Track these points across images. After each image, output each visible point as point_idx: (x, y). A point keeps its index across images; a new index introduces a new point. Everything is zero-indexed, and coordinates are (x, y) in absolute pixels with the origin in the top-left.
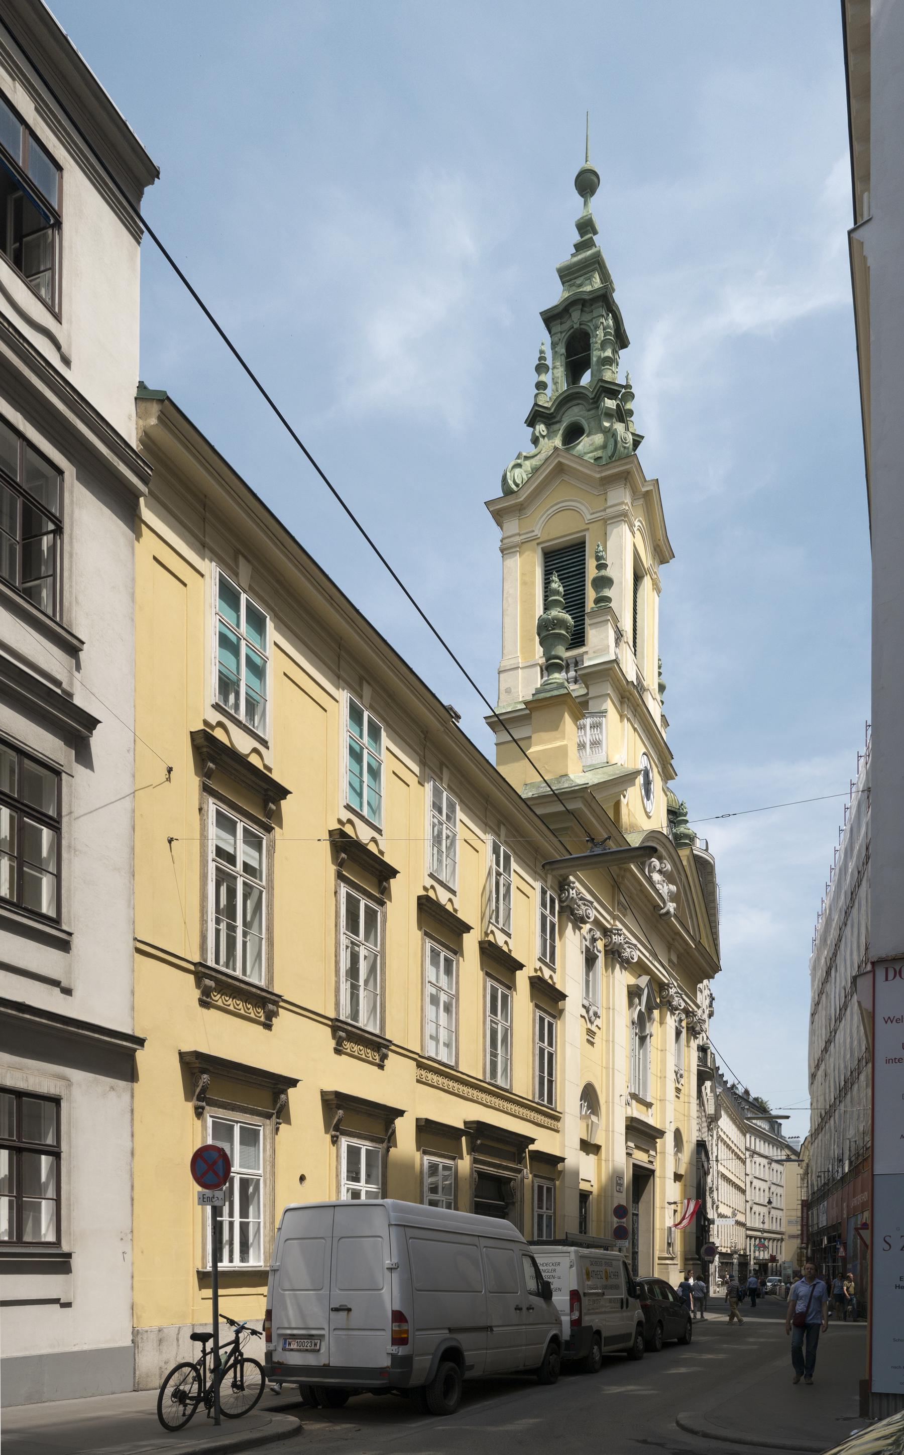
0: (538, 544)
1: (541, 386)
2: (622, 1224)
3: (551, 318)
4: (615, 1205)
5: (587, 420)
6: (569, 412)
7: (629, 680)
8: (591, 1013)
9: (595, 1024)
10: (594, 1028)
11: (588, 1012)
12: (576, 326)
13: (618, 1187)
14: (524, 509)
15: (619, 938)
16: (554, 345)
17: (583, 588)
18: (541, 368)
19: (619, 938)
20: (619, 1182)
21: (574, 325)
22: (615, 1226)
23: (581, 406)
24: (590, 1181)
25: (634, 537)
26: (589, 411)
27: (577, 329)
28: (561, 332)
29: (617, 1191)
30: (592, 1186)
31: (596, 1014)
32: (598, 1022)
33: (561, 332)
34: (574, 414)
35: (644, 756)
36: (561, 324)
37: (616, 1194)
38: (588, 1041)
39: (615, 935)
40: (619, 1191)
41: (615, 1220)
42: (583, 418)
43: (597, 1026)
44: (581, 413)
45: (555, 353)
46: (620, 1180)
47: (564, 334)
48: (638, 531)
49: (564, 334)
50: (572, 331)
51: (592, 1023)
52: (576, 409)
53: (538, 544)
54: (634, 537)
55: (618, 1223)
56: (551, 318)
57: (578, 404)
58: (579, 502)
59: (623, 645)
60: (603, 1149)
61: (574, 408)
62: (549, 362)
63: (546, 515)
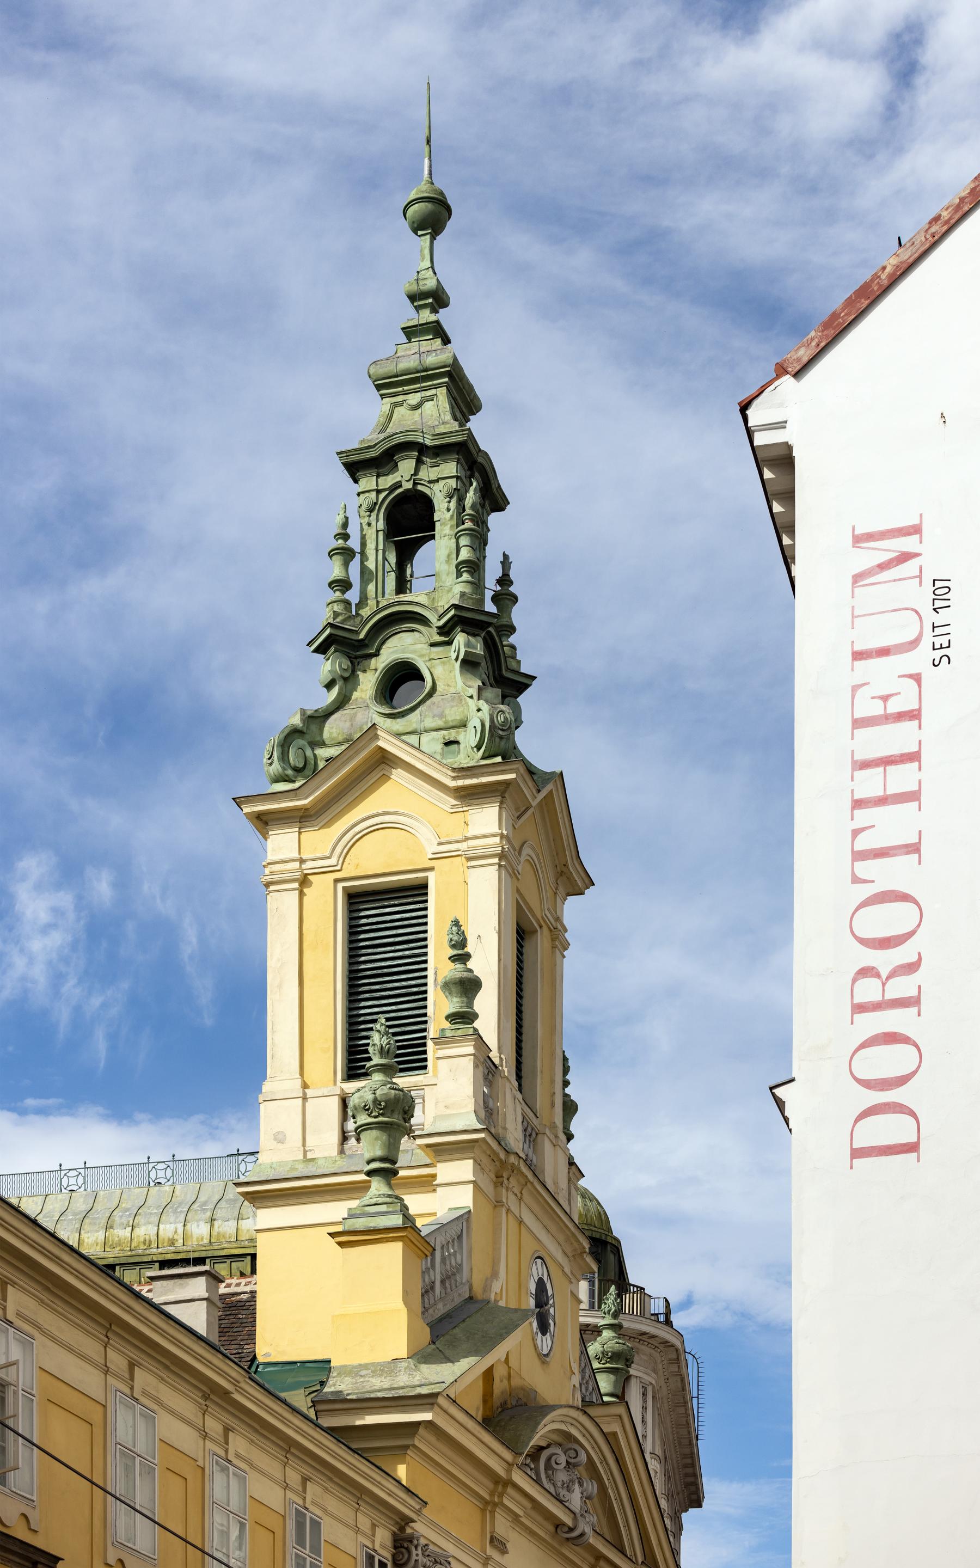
12: (408, 485)
17: (423, 966)
21: (404, 483)
33: (379, 492)
35: (539, 1261)
36: (378, 476)
47: (384, 494)
49: (384, 494)
57: (413, 631)
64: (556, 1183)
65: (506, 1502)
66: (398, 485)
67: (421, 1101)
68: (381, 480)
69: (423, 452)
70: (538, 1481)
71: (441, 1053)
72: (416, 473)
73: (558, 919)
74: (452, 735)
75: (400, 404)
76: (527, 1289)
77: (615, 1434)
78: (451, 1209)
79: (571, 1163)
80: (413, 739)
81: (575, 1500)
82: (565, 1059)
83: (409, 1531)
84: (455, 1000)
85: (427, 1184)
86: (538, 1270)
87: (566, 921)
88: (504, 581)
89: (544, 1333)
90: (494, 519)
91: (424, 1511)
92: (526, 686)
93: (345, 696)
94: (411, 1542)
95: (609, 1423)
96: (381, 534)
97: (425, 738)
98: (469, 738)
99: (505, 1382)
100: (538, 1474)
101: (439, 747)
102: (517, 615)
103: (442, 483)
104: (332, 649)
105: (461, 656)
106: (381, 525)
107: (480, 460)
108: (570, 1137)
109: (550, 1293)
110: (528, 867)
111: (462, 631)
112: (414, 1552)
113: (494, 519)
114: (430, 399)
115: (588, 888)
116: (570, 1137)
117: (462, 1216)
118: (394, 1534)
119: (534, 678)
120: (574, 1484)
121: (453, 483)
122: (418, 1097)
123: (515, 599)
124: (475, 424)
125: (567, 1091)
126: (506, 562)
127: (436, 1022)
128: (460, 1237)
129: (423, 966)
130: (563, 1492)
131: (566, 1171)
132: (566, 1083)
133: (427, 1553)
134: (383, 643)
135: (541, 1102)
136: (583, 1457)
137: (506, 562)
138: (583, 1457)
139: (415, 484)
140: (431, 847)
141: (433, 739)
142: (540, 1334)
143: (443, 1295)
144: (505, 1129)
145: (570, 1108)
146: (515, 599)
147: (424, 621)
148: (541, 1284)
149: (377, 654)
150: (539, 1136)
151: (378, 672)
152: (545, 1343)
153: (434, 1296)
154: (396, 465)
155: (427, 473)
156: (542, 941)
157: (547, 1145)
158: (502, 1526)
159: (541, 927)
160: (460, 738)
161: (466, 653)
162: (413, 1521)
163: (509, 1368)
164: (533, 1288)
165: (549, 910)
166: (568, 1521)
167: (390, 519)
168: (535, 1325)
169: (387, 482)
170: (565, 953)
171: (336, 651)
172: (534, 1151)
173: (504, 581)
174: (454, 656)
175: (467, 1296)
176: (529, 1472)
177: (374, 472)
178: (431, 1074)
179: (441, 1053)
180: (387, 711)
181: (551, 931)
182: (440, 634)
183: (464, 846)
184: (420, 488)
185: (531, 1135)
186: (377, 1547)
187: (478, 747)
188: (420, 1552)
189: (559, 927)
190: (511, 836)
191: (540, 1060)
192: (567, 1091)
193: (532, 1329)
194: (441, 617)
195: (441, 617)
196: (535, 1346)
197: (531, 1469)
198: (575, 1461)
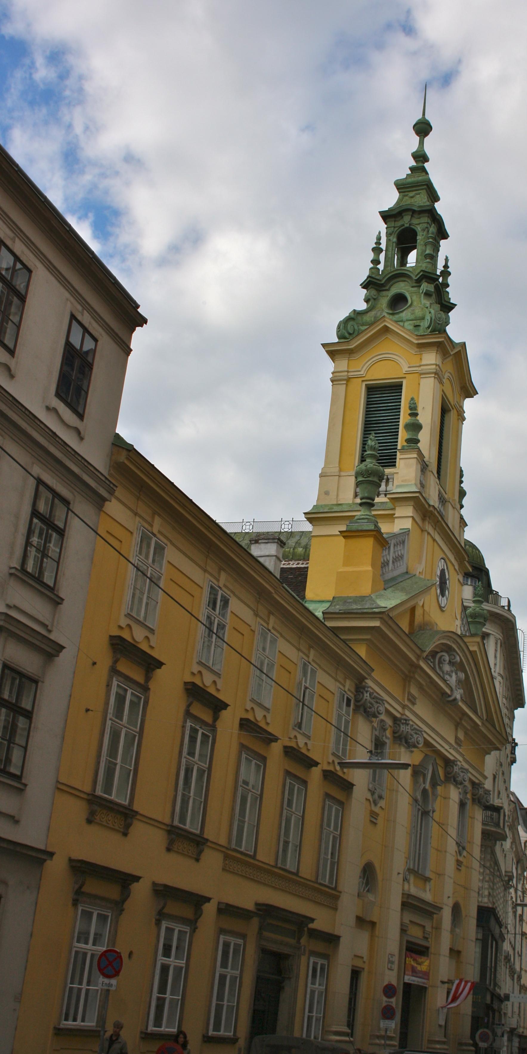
0: (363, 381)
1: (376, 262)
2: (390, 1004)
3: (386, 216)
4: (386, 983)
5: (411, 293)
6: (396, 285)
7: (431, 503)
8: (376, 796)
9: (379, 805)
10: (377, 810)
11: (373, 793)
12: (407, 225)
13: (390, 965)
14: (354, 353)
15: (407, 727)
16: (388, 235)
17: (398, 420)
18: (377, 250)
19: (407, 727)
20: (391, 959)
22: (384, 1004)
23: (406, 283)
24: (362, 958)
25: (443, 391)
26: (413, 287)
27: (407, 227)
28: (394, 227)
29: (388, 969)
30: (364, 962)
31: (381, 797)
32: (382, 803)
33: (394, 227)
34: (400, 287)
35: (443, 561)
36: (395, 221)
37: (387, 972)
38: (371, 821)
39: (403, 724)
40: (391, 969)
41: (385, 999)
42: (408, 291)
43: (381, 807)
44: (407, 287)
45: (388, 241)
46: (392, 957)
47: (396, 229)
48: (448, 380)
49: (396, 229)
50: (403, 227)
51: (376, 804)
52: (402, 284)
53: (363, 381)
54: (443, 391)
55: (386, 1001)
56: (386, 216)
57: (405, 281)
58: (399, 356)
59: (429, 474)
60: (377, 925)
61: (401, 283)
62: (383, 246)
63: (371, 361)
64: (453, 526)
65: (417, 676)
66: (403, 225)
67: (392, 480)
68: (396, 223)
69: (413, 212)
70: (433, 669)
71: (402, 456)
72: (410, 221)
73: (462, 407)
74: (417, 323)
75: (407, 196)
76: (436, 573)
77: (475, 651)
78: (401, 529)
79: (462, 518)
80: (401, 324)
81: (453, 680)
82: (461, 471)
83: (364, 684)
84: (410, 433)
85: (391, 517)
86: (441, 564)
87: (465, 408)
88: (446, 266)
89: (443, 595)
90: (442, 242)
91: (373, 674)
92: (452, 308)
93: (374, 306)
94: (364, 689)
95: (473, 646)
96: (394, 244)
97: (406, 324)
98: (426, 323)
99: (421, 617)
100: (434, 665)
101: (411, 327)
102: (450, 280)
103: (421, 225)
104: (370, 287)
105: (424, 291)
106: (395, 240)
107: (438, 217)
108: (462, 507)
109: (447, 577)
110: (448, 382)
111: (426, 281)
112: (365, 695)
113: (442, 242)
114: (419, 194)
115: (475, 395)
116: (462, 507)
117: (405, 532)
118: (356, 685)
119: (456, 305)
120: (452, 673)
121: (425, 225)
122: (391, 478)
123: (449, 274)
124: (437, 205)
125: (462, 485)
126: (447, 260)
127: (401, 442)
128: (404, 542)
129: (398, 420)
130: (447, 677)
131: (459, 521)
132: (461, 482)
133: (373, 696)
134: (392, 285)
135: (448, 487)
136: (458, 659)
137: (447, 260)
138: (458, 659)
139: (410, 225)
140: (405, 369)
141: (410, 324)
142: (441, 596)
143: (393, 568)
144: (429, 495)
145: (462, 494)
146: (449, 274)
147: (409, 277)
148: (443, 572)
149: (388, 290)
150: (447, 503)
151: (388, 297)
152: (443, 601)
153: (388, 568)
154: (403, 217)
155: (415, 221)
156: (453, 415)
157: (450, 508)
158: (414, 691)
159: (453, 409)
160: (421, 324)
161: (426, 290)
162: (367, 679)
163: (424, 610)
164: (439, 573)
165: (457, 402)
166: (448, 691)
167: (399, 238)
168: (439, 591)
169: (399, 224)
170: (464, 422)
171: (371, 288)
172: (444, 508)
173: (446, 266)
174: (421, 292)
175: (405, 571)
176: (430, 662)
177: (393, 219)
178: (397, 468)
179: (402, 456)
180: (391, 312)
181: (457, 411)
182: (416, 283)
183: (420, 369)
184: (412, 226)
185: (442, 500)
186: (346, 690)
187: (429, 327)
188: (368, 695)
189: (461, 410)
190: (441, 365)
191: (448, 469)
192: (462, 485)
193: (437, 594)
194: (416, 276)
195: (416, 276)
196: (438, 601)
197: (431, 662)
198: (454, 661)
